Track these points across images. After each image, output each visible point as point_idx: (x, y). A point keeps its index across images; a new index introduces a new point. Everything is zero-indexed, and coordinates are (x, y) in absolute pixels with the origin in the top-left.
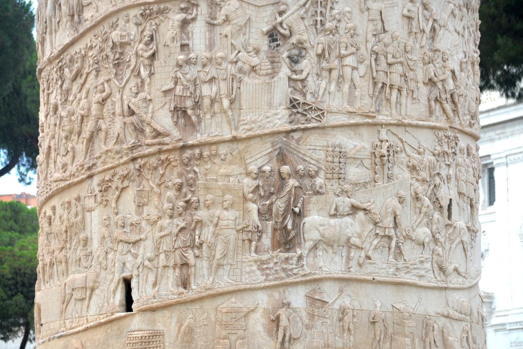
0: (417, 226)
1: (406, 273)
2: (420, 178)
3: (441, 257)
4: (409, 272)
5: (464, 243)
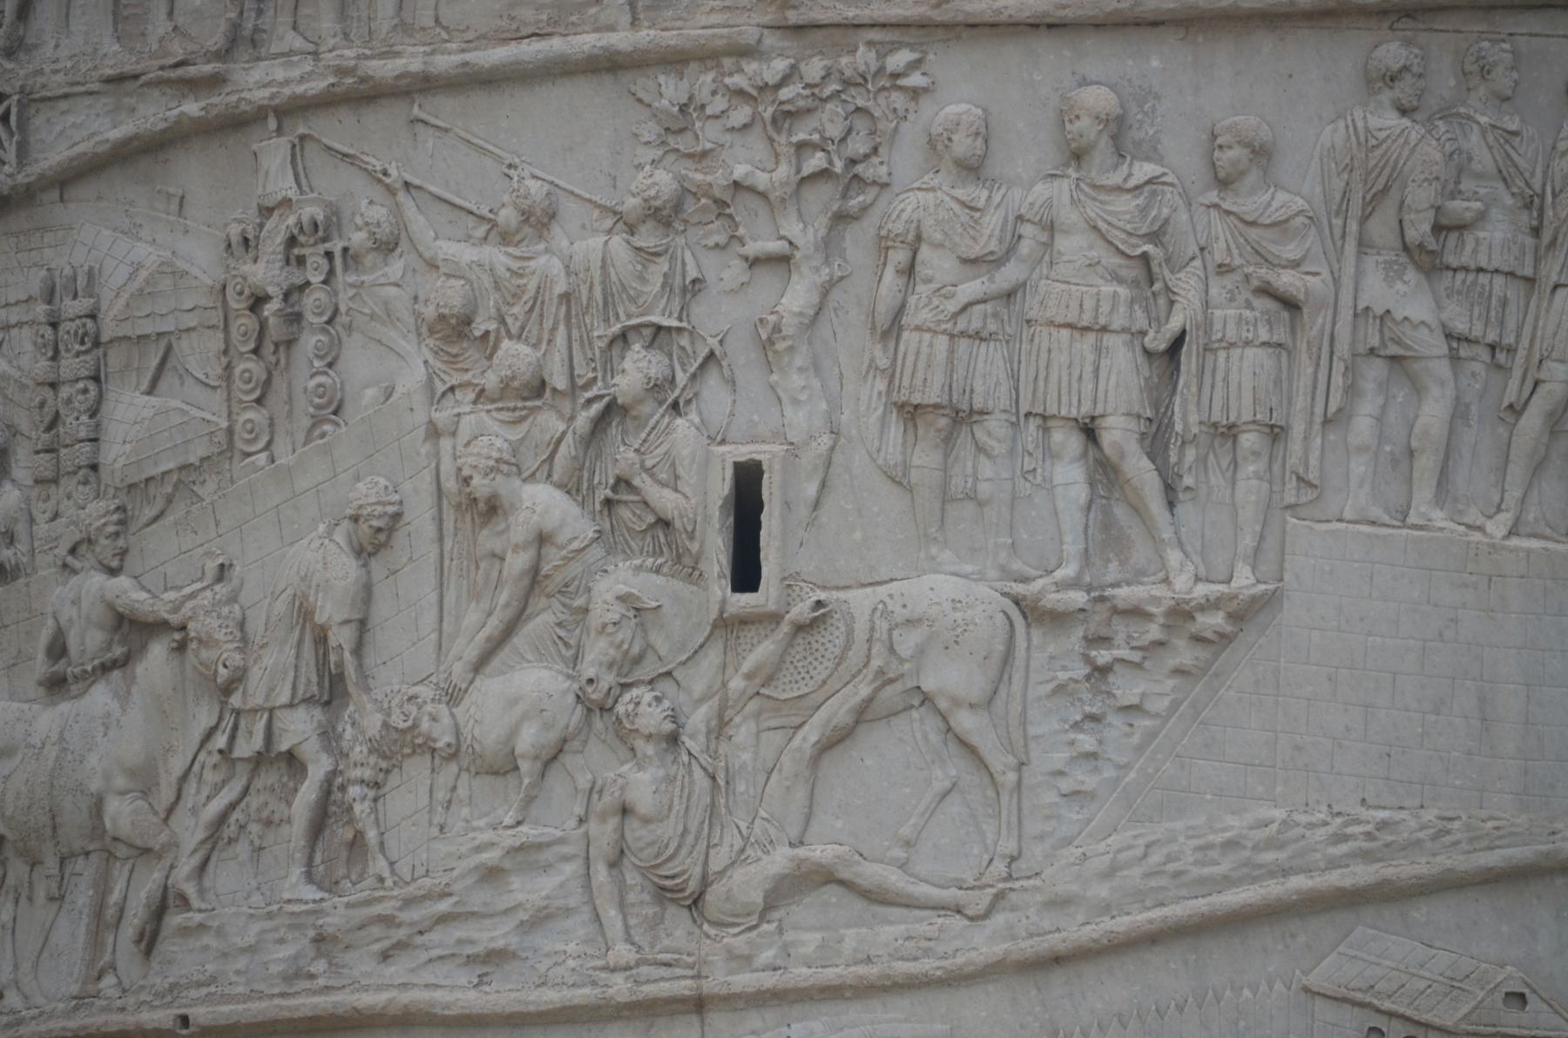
0: (480, 665)
1: (385, 956)
2: (491, 381)
3: (646, 821)
4: (401, 946)
5: (943, 704)
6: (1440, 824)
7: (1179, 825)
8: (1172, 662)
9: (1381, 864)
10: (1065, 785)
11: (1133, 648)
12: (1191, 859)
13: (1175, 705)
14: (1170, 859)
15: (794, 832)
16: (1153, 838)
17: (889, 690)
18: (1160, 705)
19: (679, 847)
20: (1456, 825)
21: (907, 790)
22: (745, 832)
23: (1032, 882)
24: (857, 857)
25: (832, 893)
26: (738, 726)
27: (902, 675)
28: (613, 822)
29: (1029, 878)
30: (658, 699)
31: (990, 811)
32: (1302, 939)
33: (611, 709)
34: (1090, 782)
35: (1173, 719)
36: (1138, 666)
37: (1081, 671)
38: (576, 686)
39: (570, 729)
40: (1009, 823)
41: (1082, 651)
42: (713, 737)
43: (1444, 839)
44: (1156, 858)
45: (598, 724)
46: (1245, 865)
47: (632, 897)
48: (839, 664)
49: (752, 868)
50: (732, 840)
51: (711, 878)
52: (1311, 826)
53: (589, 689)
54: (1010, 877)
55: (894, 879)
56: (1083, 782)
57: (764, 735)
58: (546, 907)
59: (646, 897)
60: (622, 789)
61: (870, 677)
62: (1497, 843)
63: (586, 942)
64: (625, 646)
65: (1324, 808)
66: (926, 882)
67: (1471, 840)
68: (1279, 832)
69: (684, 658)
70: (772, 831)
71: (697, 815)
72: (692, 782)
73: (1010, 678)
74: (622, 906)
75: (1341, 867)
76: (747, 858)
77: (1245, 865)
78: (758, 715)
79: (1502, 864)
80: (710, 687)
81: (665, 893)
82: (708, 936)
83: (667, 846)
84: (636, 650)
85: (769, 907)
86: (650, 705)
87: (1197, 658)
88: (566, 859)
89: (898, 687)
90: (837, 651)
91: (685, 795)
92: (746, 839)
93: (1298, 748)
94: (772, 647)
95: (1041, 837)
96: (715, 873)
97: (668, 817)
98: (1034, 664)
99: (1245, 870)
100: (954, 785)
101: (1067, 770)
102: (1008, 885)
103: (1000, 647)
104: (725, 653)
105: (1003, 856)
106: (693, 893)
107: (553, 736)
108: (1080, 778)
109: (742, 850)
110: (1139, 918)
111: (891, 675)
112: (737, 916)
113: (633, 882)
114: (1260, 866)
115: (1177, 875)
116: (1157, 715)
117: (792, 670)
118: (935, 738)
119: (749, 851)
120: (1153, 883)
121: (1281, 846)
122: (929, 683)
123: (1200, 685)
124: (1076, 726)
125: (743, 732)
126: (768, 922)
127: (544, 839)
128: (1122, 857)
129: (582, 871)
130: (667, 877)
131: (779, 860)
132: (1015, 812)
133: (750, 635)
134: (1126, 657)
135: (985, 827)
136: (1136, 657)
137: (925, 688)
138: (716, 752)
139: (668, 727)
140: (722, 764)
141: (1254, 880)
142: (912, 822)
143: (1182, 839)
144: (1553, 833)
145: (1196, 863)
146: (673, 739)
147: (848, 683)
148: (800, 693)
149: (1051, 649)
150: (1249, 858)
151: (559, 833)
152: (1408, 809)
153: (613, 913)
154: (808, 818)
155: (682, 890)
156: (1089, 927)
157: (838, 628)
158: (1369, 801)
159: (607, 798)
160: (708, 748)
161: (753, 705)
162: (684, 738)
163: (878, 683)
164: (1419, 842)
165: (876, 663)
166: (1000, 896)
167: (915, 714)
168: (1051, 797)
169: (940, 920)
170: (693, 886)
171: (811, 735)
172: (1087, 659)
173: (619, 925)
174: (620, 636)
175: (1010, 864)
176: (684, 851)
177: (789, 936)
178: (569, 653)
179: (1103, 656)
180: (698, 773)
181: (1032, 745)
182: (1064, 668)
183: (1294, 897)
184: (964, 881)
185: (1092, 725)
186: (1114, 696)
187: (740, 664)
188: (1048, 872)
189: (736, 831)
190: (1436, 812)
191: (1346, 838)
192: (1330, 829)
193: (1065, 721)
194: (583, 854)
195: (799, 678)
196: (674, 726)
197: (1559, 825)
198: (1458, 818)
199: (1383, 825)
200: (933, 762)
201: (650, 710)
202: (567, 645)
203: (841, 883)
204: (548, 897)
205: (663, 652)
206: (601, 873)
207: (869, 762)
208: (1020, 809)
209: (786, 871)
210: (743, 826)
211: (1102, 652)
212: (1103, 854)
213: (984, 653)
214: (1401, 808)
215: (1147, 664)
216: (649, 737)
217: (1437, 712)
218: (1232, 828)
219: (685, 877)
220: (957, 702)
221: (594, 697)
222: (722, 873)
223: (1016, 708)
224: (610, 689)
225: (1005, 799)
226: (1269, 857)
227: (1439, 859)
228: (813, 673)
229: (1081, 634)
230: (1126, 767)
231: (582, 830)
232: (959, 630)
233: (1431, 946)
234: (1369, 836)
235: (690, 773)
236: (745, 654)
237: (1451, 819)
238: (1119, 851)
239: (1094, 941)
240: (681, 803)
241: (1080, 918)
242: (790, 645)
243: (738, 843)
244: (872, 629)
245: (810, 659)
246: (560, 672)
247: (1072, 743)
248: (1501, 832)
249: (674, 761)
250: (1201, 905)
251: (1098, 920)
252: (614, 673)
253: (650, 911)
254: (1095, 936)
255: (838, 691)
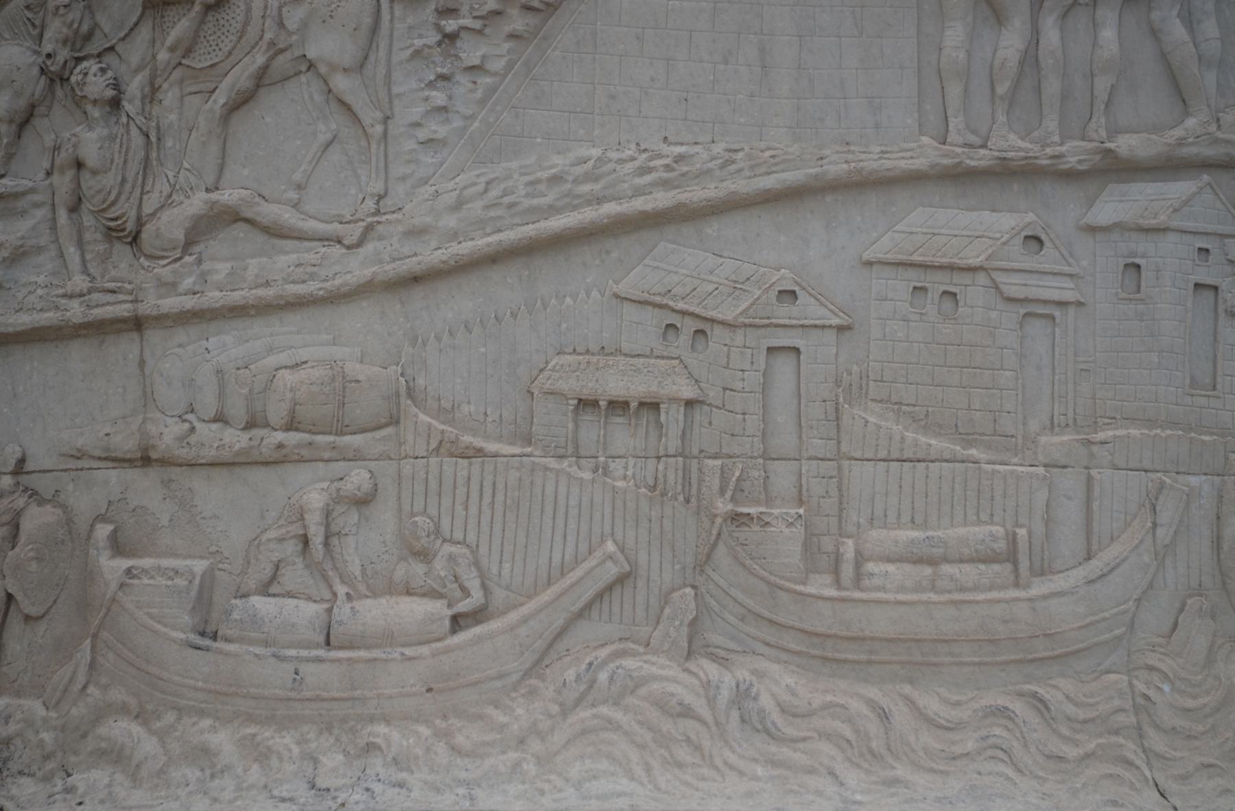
3: (95, 173)
6: (727, 155)
7: (514, 165)
8: (508, 29)
9: (678, 190)
10: (422, 134)
11: (475, 17)
12: (523, 193)
13: (510, 65)
14: (505, 193)
15: (210, 180)
16: (492, 176)
17: (281, 58)
18: (497, 65)
19: (119, 194)
20: (740, 155)
21: (299, 142)
22: (172, 180)
23: (395, 216)
24: (257, 199)
25: (240, 230)
26: (166, 91)
27: (291, 46)
28: (70, 174)
29: (393, 212)
30: (103, 70)
31: (364, 158)
32: (614, 255)
33: (68, 79)
34: (442, 131)
35: (510, 76)
36: (480, 32)
37: (433, 38)
38: (40, 60)
39: (36, 96)
40: (377, 168)
41: (434, 20)
42: (147, 101)
43: (729, 168)
44: (494, 193)
45: (59, 93)
46: (567, 195)
47: (88, 236)
48: (241, 38)
49: (175, 210)
50: (162, 187)
51: (144, 219)
52: (621, 161)
53: (49, 63)
54: (378, 212)
55: (288, 217)
56: (435, 132)
57: (187, 99)
58: (22, 246)
59: (99, 236)
60: (75, 146)
61: (264, 47)
62: (774, 169)
63: (54, 274)
64: (76, 26)
65: (633, 146)
66: (315, 218)
67: (752, 167)
68: (594, 167)
69: (122, 35)
70: (193, 179)
71: (134, 167)
72: (129, 140)
73: (378, 46)
74: (80, 244)
75: (645, 194)
76: (172, 202)
77: (567, 195)
78: (181, 81)
79: (778, 186)
80: (143, 59)
81: (113, 233)
82: (143, 268)
83: (110, 193)
84: (85, 28)
85: (189, 243)
86: (95, 75)
87: (527, 24)
88: (37, 205)
89: (288, 55)
90: (239, 26)
91: (124, 150)
92: (173, 187)
93: (612, 97)
94: (187, 24)
95: (403, 178)
96: (147, 215)
97: (111, 169)
98: (396, 34)
99: (567, 200)
100: (335, 137)
101: (423, 122)
102: (375, 219)
103: (368, 20)
104: (154, 29)
105: (373, 195)
106: (131, 232)
107: (22, 103)
108: (432, 128)
109: (170, 196)
110: (480, 243)
111: (281, 46)
112: (166, 250)
113: (88, 224)
114: (579, 196)
115: (511, 206)
116: (495, 74)
117: (205, 43)
118: (318, 98)
119: (174, 197)
120: (492, 213)
121: (597, 179)
122: (311, 53)
123: (530, 48)
124: (431, 85)
125: (169, 96)
126: (191, 255)
127: (19, 189)
128: (467, 193)
129: (50, 216)
130: (112, 219)
131: (196, 203)
132: (382, 158)
133: (172, 14)
134: (470, 26)
135: (359, 171)
136: (477, 25)
137: (309, 56)
138: (150, 114)
139: (110, 93)
140: (154, 124)
141: (575, 208)
142: (303, 168)
143: (516, 176)
144: (822, 158)
145: (527, 195)
146: (115, 104)
147: (248, 53)
148: (212, 62)
149: (410, 20)
150: (570, 190)
151: (30, 184)
152: (702, 144)
153: (72, 250)
154: (221, 168)
155: (124, 230)
156: (440, 251)
157: (238, 7)
158: (671, 139)
159: (63, 154)
160: (143, 110)
161: (177, 74)
162: (124, 103)
163: (271, 52)
164: (709, 172)
165: (268, 36)
166: (369, 228)
167: (303, 78)
168: (410, 145)
169: (323, 250)
170: (130, 226)
171: (221, 98)
172: (438, 28)
173: (77, 259)
174: (70, 17)
175: (378, 201)
176: (123, 197)
177: (206, 266)
178: (35, 32)
179: (451, 25)
180: (134, 132)
181: (396, 102)
182: (421, 36)
183: (605, 221)
184: (343, 216)
185: (445, 83)
186: (460, 58)
187: (165, 39)
188: (408, 207)
189: (165, 180)
190: (723, 145)
191: (650, 170)
192: (637, 164)
193: (421, 80)
194: (51, 202)
195: (211, 49)
196: (115, 92)
197: (827, 152)
198: (742, 149)
199: (680, 159)
200: (318, 118)
201: (95, 79)
202: (33, 25)
203: (247, 221)
204: (23, 238)
205: (107, 30)
206: (63, 217)
207: (268, 120)
208: (386, 156)
209: (203, 212)
210: (170, 174)
211: (450, 22)
212: (452, 191)
213: (354, 26)
214: (696, 143)
215: (487, 31)
216: (95, 102)
217: (726, 62)
218: (557, 165)
219: (124, 219)
220: (333, 68)
221: (52, 69)
222: (153, 215)
223: (382, 70)
224: (66, 62)
225: (374, 146)
226: (586, 188)
227: (725, 184)
228: (221, 45)
229: (433, 7)
230: (472, 117)
231: (47, 182)
232: (334, 6)
233: (721, 256)
234: (668, 168)
235: (128, 132)
236: (168, 30)
237: (736, 151)
238: (465, 188)
239: (443, 262)
240: (120, 158)
241: (434, 244)
242: (202, 22)
243: (166, 189)
244: (266, 7)
245: (219, 34)
246: (28, 48)
247: (427, 99)
248: (777, 160)
249: (116, 123)
250: (530, 230)
251: (447, 245)
252: (68, 48)
253: (101, 247)
254: (444, 258)
255: (241, 60)
